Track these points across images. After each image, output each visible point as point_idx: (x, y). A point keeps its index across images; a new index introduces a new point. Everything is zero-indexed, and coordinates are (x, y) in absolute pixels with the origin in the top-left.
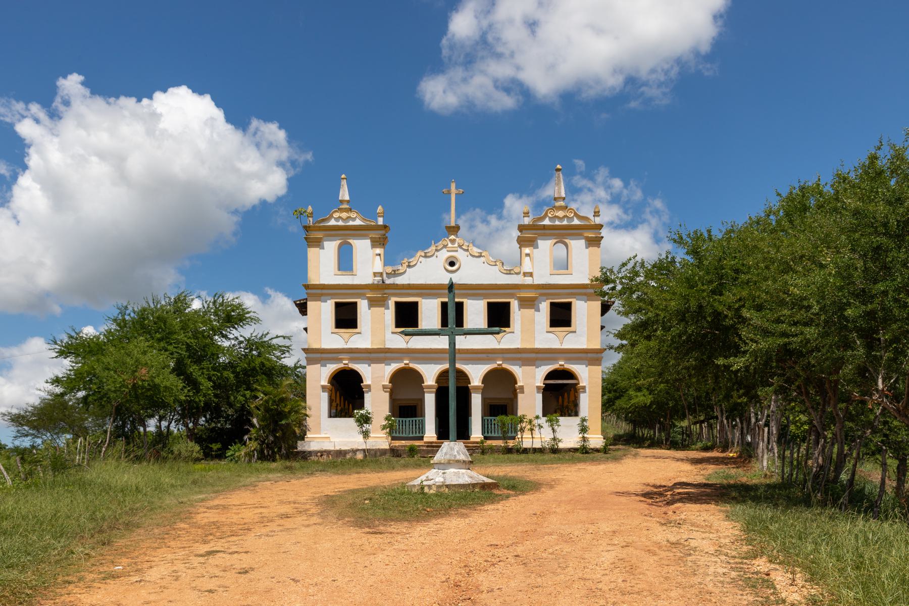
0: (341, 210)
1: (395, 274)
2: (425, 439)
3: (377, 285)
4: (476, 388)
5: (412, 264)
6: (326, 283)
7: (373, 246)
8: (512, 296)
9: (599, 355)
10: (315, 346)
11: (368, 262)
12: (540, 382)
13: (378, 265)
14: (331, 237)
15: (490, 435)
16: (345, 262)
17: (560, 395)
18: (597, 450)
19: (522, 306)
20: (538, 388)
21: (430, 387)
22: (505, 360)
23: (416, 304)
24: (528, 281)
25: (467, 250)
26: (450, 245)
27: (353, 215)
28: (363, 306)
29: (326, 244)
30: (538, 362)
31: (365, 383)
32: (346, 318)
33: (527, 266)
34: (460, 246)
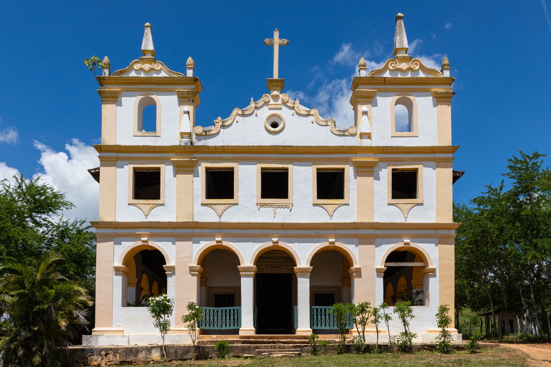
0: (144, 61)
1: (206, 135)
2: (241, 333)
3: (185, 147)
4: (303, 271)
5: (226, 124)
6: (122, 144)
7: (181, 103)
8: (346, 161)
10: (107, 218)
11: (175, 120)
12: (380, 264)
13: (187, 125)
14: (131, 92)
15: (319, 327)
16: (148, 120)
17: (403, 281)
19: (358, 174)
20: (378, 270)
21: (247, 269)
22: (338, 237)
23: (233, 168)
24: (366, 143)
25: (293, 108)
26: (272, 102)
27: (158, 66)
28: (167, 173)
29: (124, 100)
30: (378, 240)
31: (168, 264)
32: (147, 186)
33: (364, 125)
34: (284, 103)
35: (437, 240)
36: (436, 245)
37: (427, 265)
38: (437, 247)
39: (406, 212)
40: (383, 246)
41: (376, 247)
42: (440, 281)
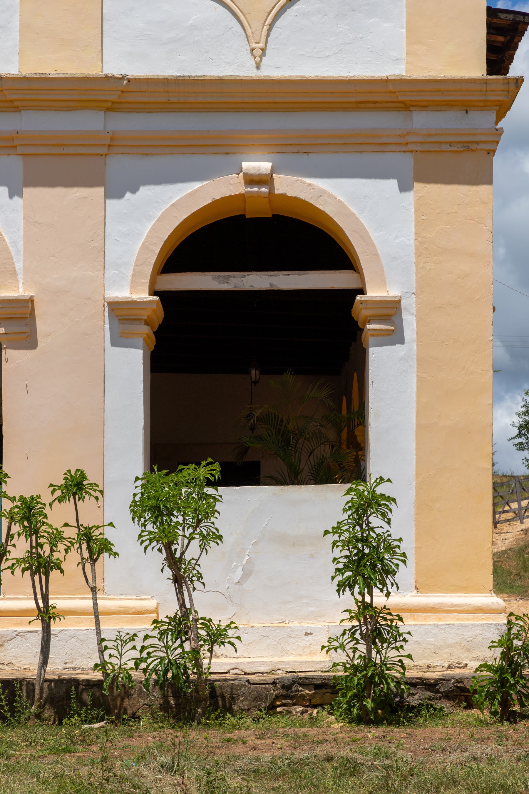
9: (482, 120)
12: (129, 279)
18: (460, 693)
30: (117, 165)
35: (406, 161)
36: (404, 187)
37: (362, 291)
38: (410, 197)
39: (257, 26)
40: (145, 191)
41: (108, 196)
42: (421, 361)
